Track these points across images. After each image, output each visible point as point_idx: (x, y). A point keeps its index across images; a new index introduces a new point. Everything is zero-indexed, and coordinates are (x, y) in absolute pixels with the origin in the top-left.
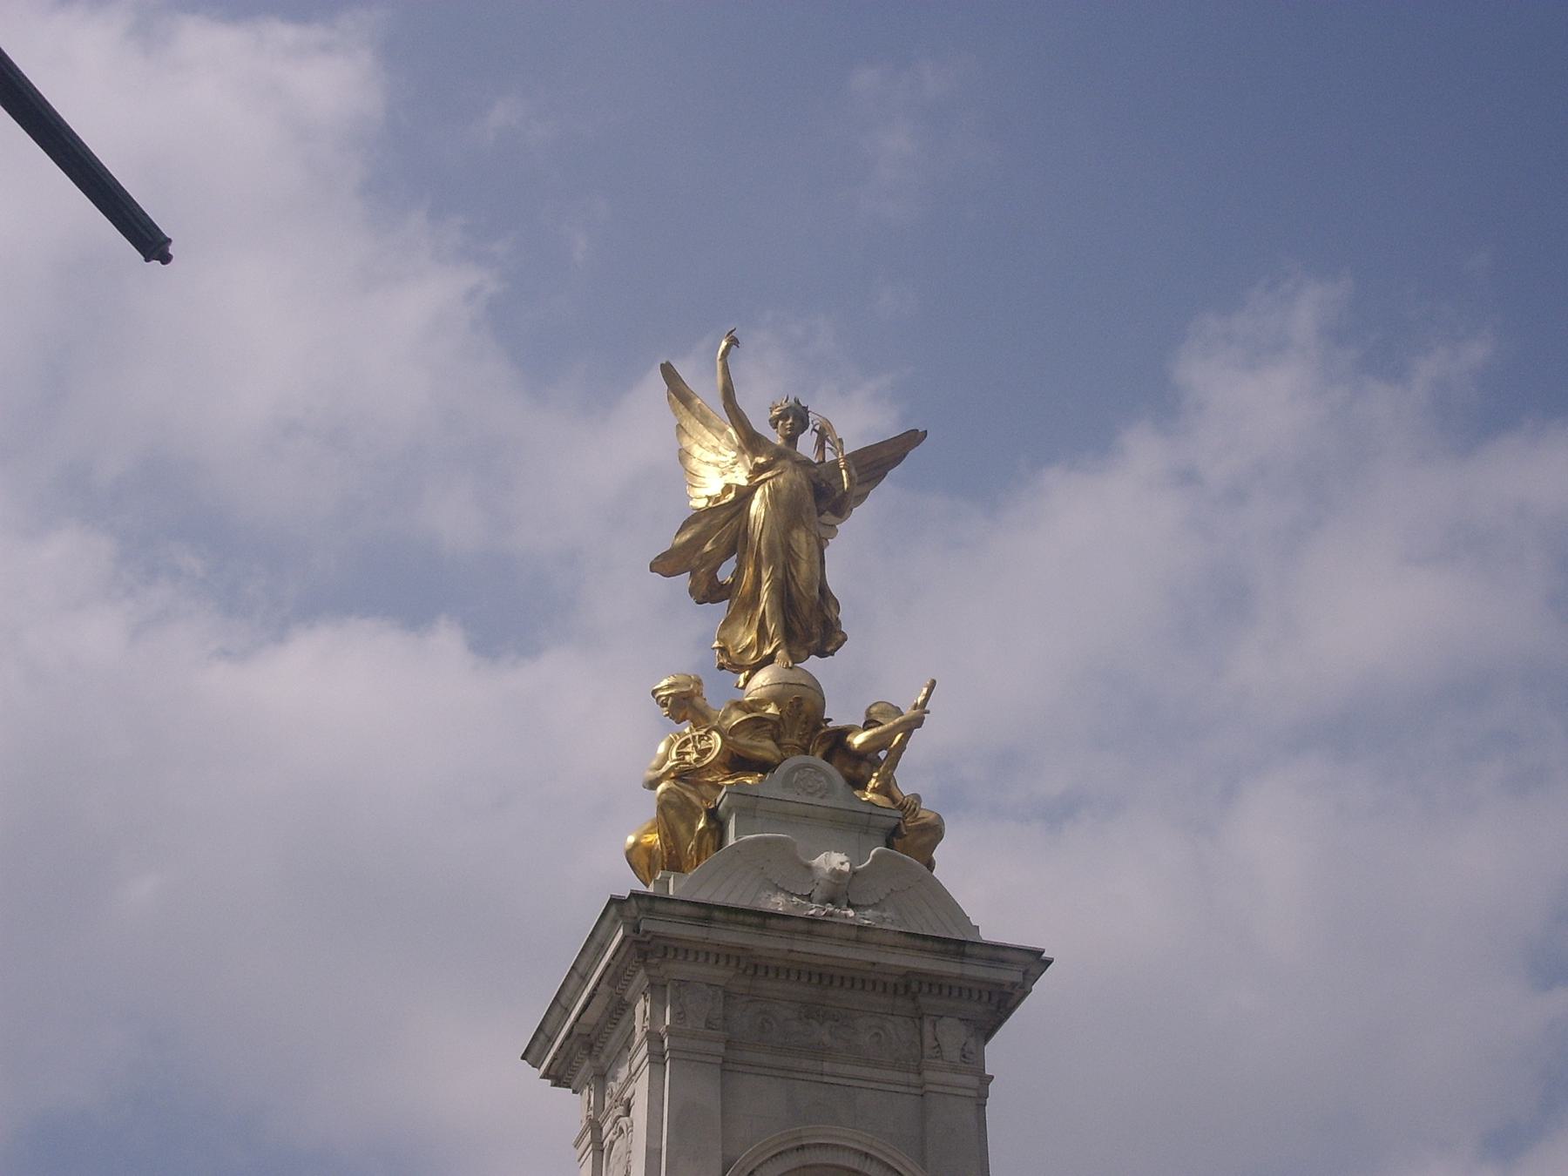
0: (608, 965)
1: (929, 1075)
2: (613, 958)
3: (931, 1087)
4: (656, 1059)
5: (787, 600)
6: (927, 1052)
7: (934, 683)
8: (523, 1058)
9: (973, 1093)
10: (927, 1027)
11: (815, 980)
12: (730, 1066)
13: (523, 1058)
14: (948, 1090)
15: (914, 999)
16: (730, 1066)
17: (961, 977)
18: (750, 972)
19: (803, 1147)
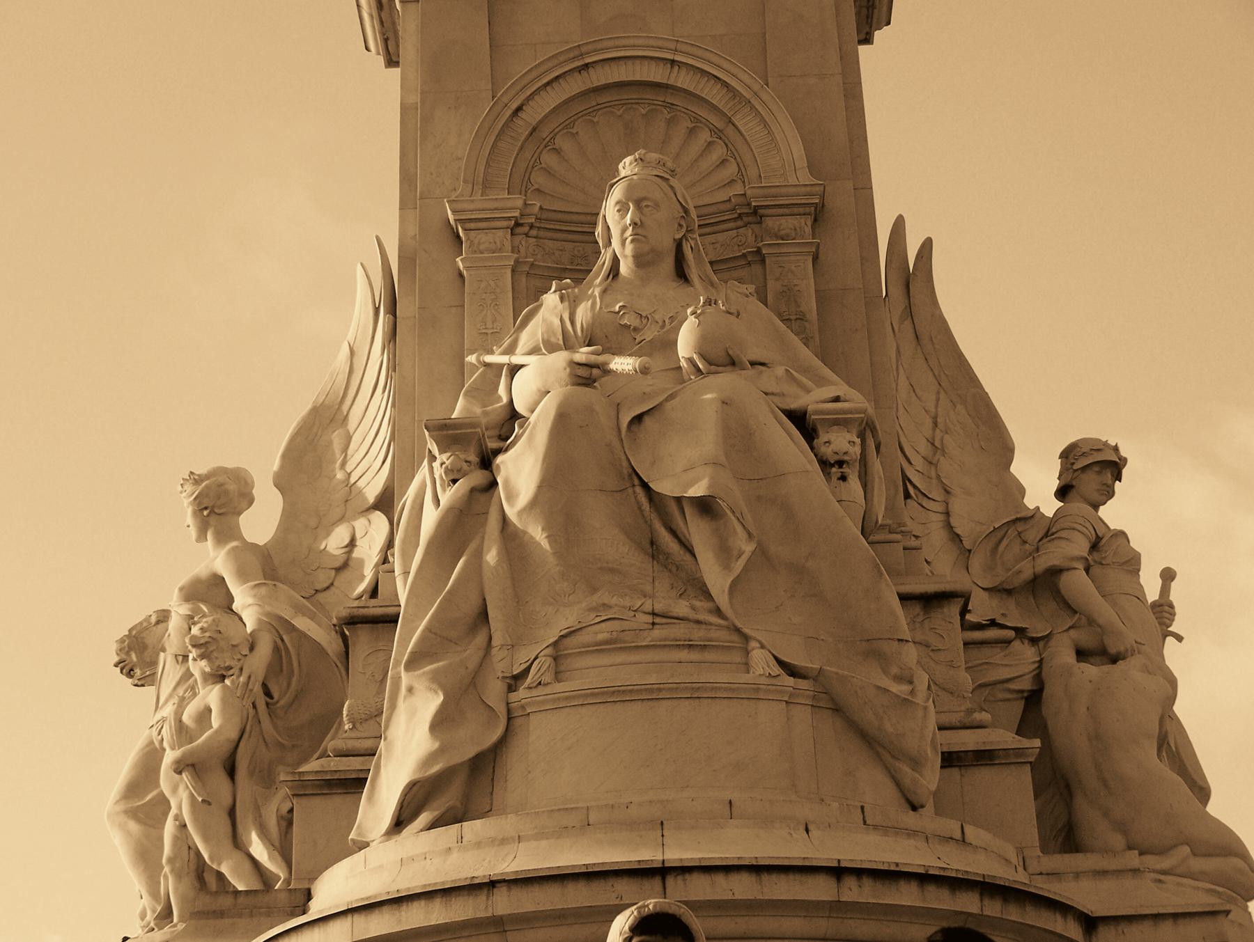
19: (586, 66)
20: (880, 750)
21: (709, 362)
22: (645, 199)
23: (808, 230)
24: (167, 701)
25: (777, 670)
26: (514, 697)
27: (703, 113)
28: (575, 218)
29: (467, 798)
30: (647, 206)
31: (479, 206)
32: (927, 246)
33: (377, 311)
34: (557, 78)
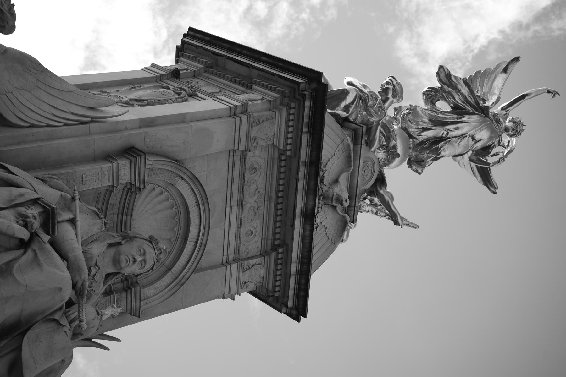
1: (235, 266)
3: (229, 267)
4: (233, 113)
6: (246, 262)
7: (415, 226)
8: (190, 29)
12: (231, 154)
13: (190, 29)
14: (228, 278)
16: (231, 154)
19: (198, 205)
22: (145, 263)
28: (131, 205)
30: (142, 265)
31: (142, 169)
32: (107, 349)
34: (195, 193)
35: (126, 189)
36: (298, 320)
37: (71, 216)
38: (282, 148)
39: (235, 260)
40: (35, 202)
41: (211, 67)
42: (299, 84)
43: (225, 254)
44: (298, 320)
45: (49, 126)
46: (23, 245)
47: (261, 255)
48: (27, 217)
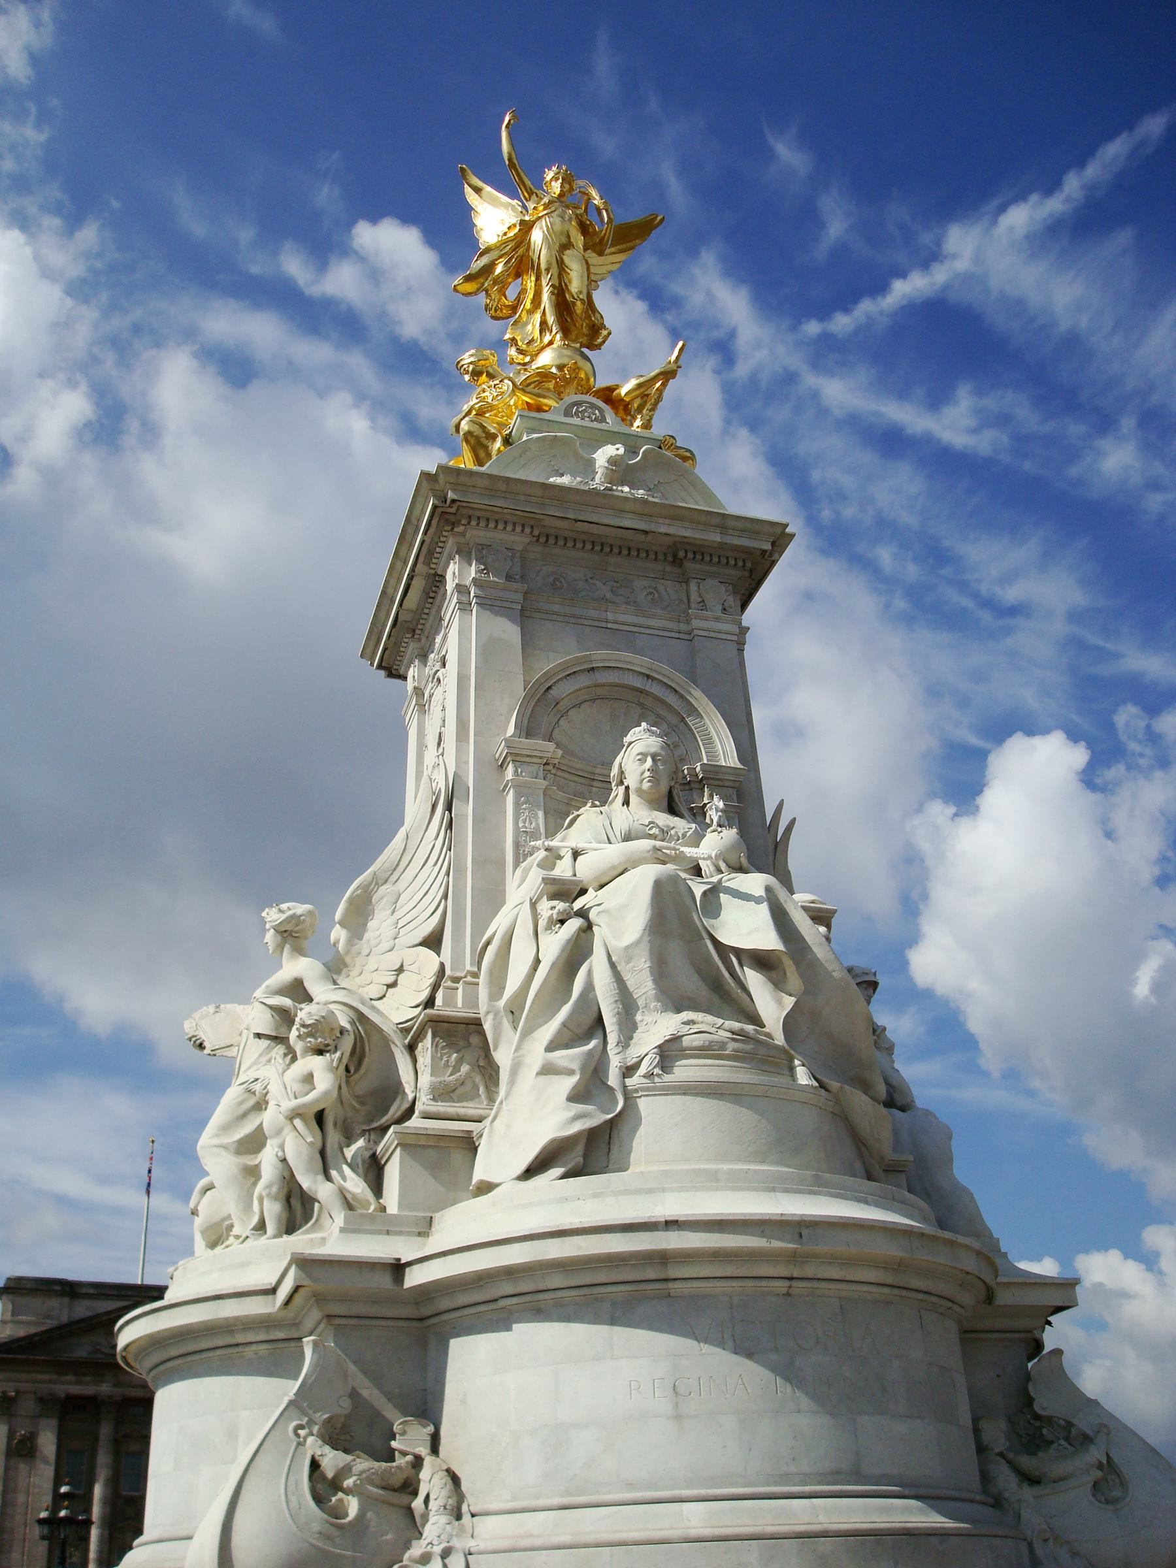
0: (422, 542)
1: (696, 623)
2: (425, 533)
3: (696, 632)
4: (464, 607)
5: (563, 306)
6: (693, 605)
9: (735, 638)
10: (693, 586)
11: (598, 548)
12: (528, 614)
15: (681, 566)
17: (722, 545)
18: (542, 540)
19: (593, 669)
20: (863, 1149)
21: (729, 866)
23: (735, 797)
24: (249, 1068)
25: (816, 1084)
26: (628, 1081)
27: (664, 713)
29: (586, 1155)
32: (793, 821)
33: (434, 807)
35: (554, 771)
36: (792, 536)
37: (568, 857)
38: (527, 540)
39: (688, 622)
40: (533, 905)
41: (414, 631)
42: (435, 507)
43: (677, 635)
44: (792, 536)
45: (448, 874)
46: (589, 927)
47: (687, 582)
48: (551, 916)
